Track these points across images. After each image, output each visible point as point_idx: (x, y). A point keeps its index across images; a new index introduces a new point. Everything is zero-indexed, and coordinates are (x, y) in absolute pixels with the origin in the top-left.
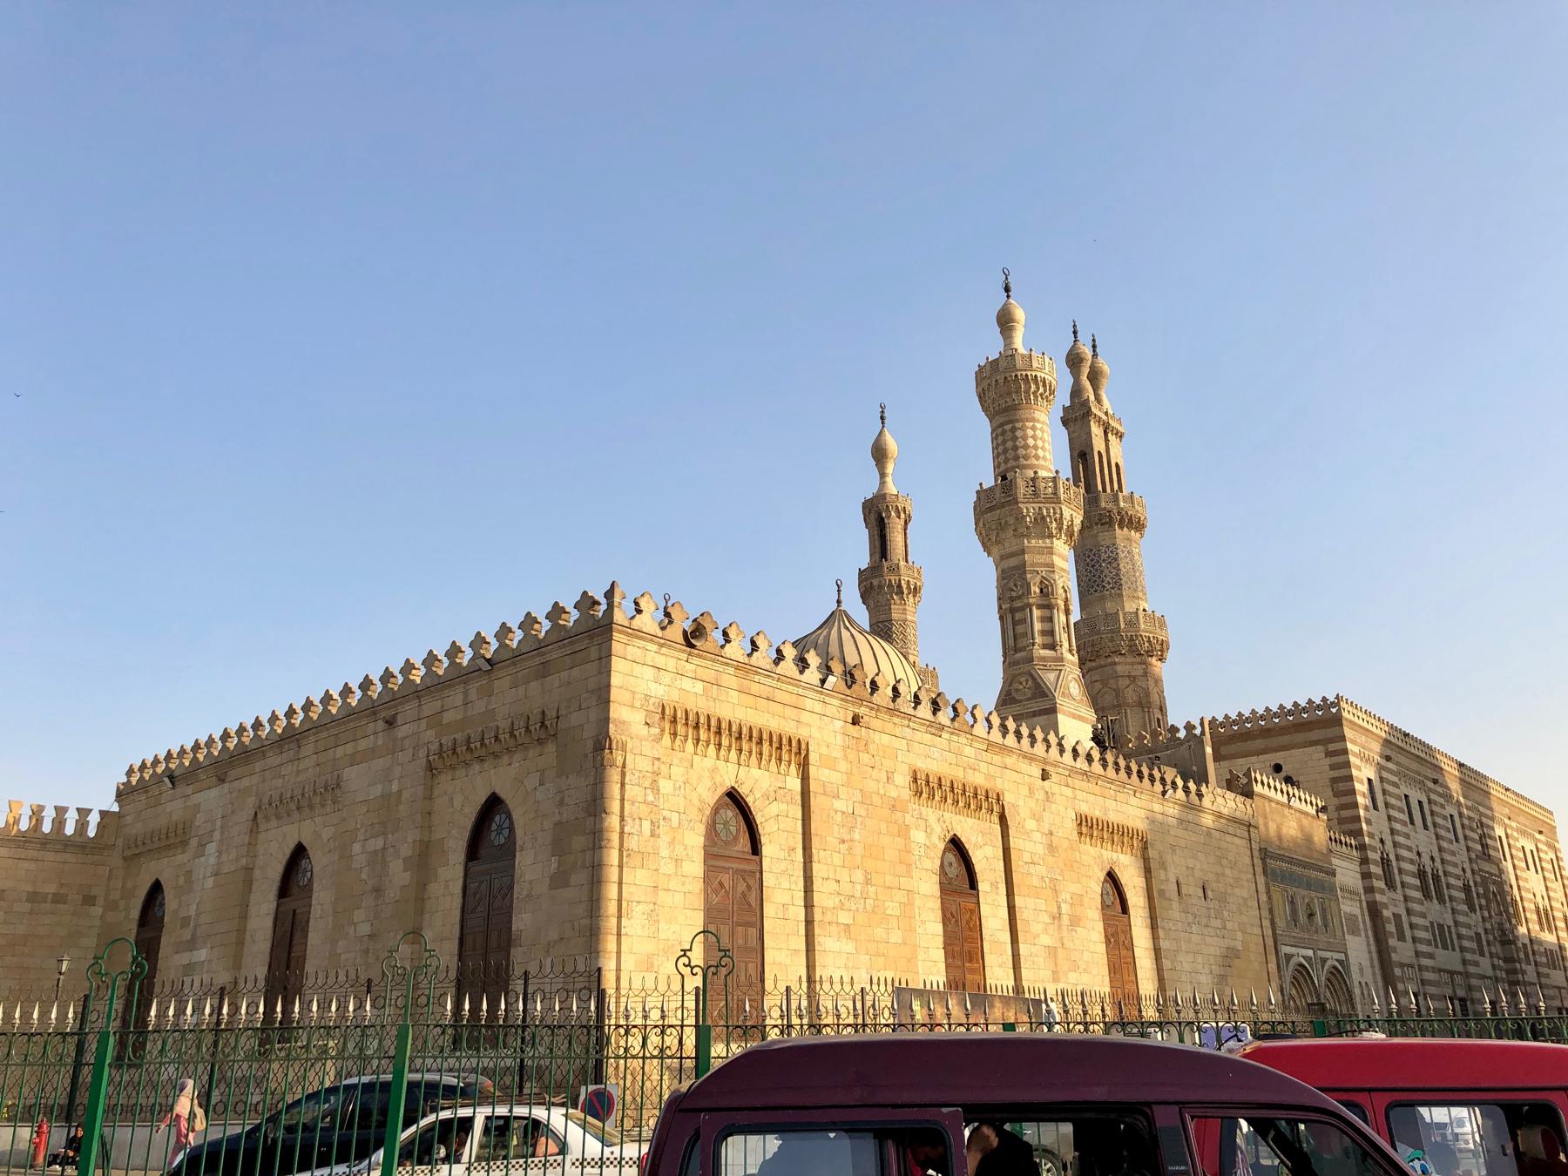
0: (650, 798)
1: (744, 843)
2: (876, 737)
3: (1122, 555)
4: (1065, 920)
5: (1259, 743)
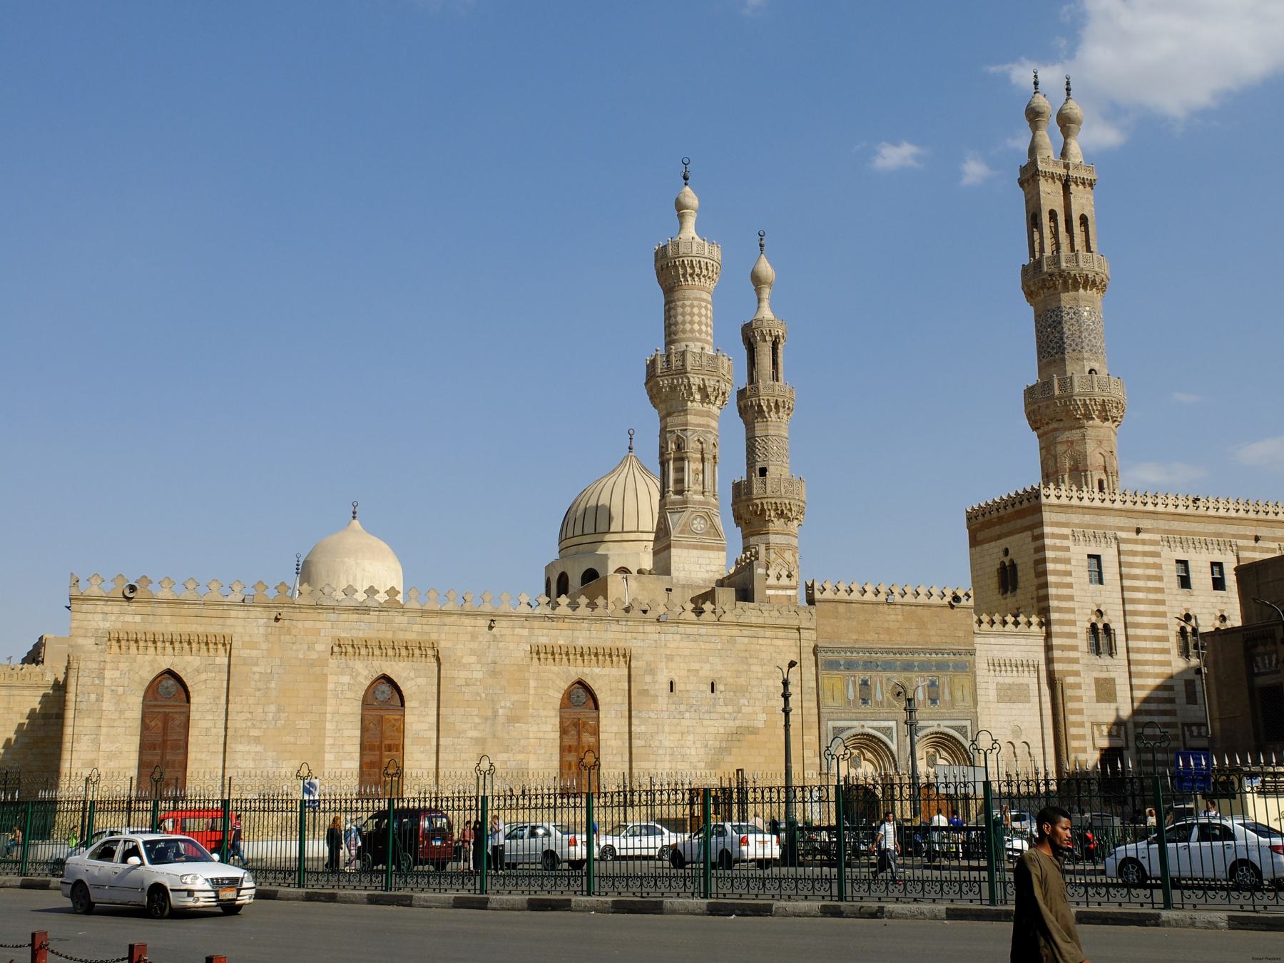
0: (97, 682)
1: (183, 696)
2: (300, 624)
3: (1066, 318)
4: (501, 720)
5: (996, 530)
